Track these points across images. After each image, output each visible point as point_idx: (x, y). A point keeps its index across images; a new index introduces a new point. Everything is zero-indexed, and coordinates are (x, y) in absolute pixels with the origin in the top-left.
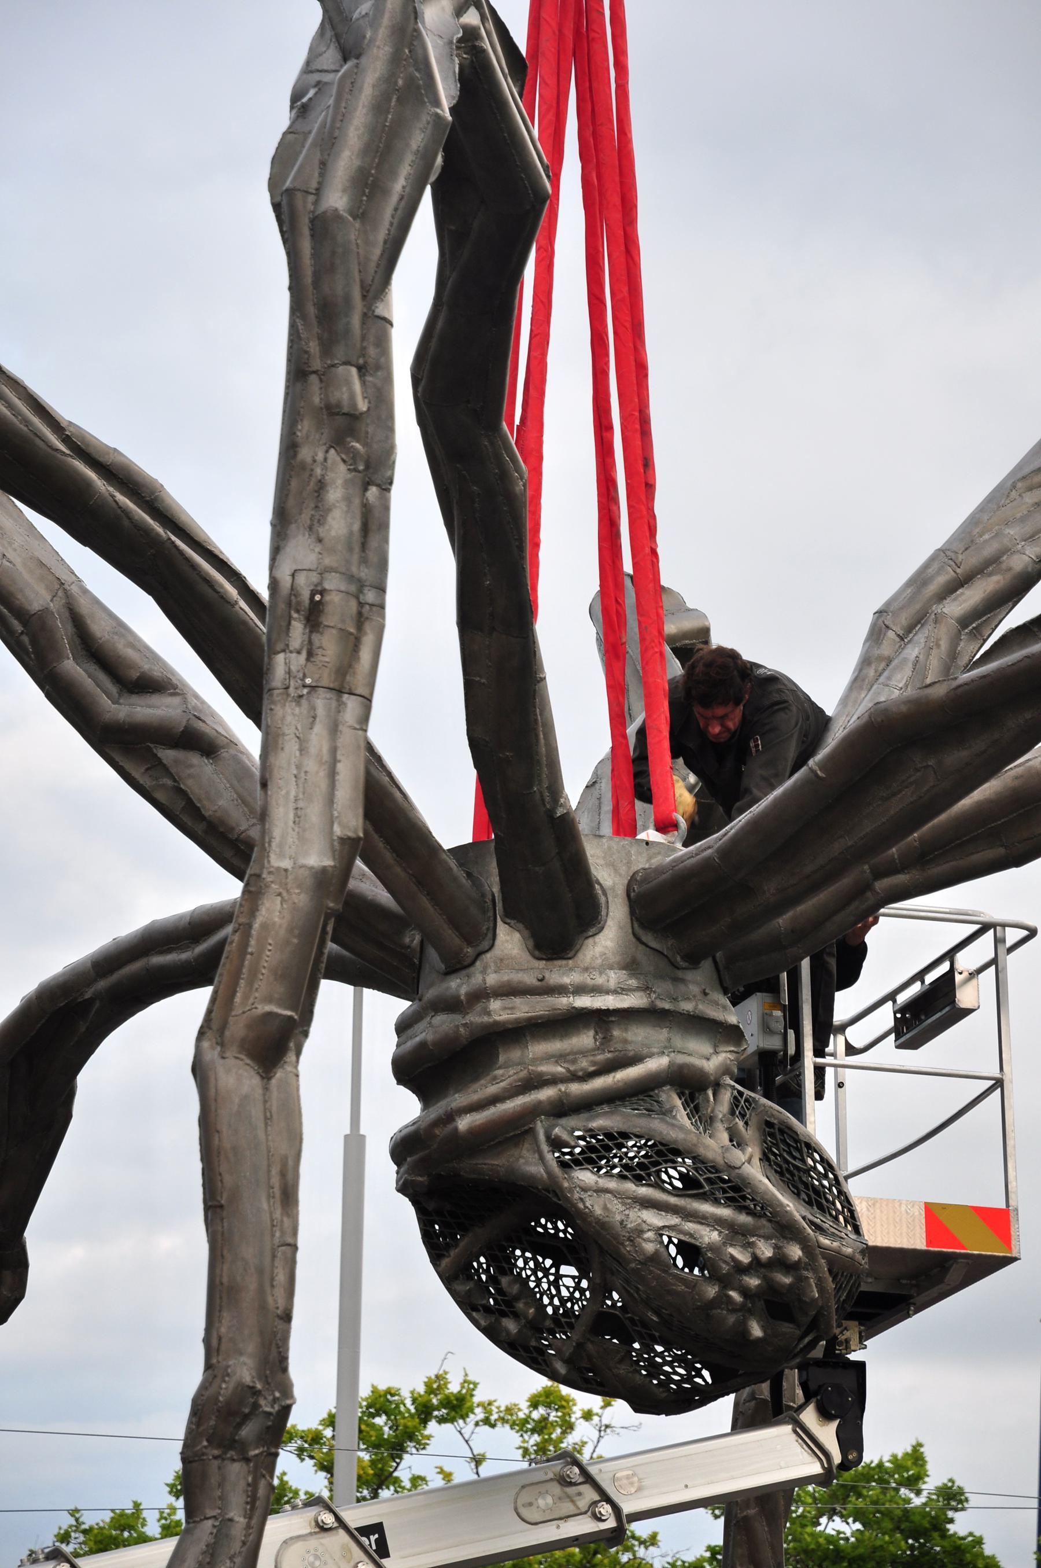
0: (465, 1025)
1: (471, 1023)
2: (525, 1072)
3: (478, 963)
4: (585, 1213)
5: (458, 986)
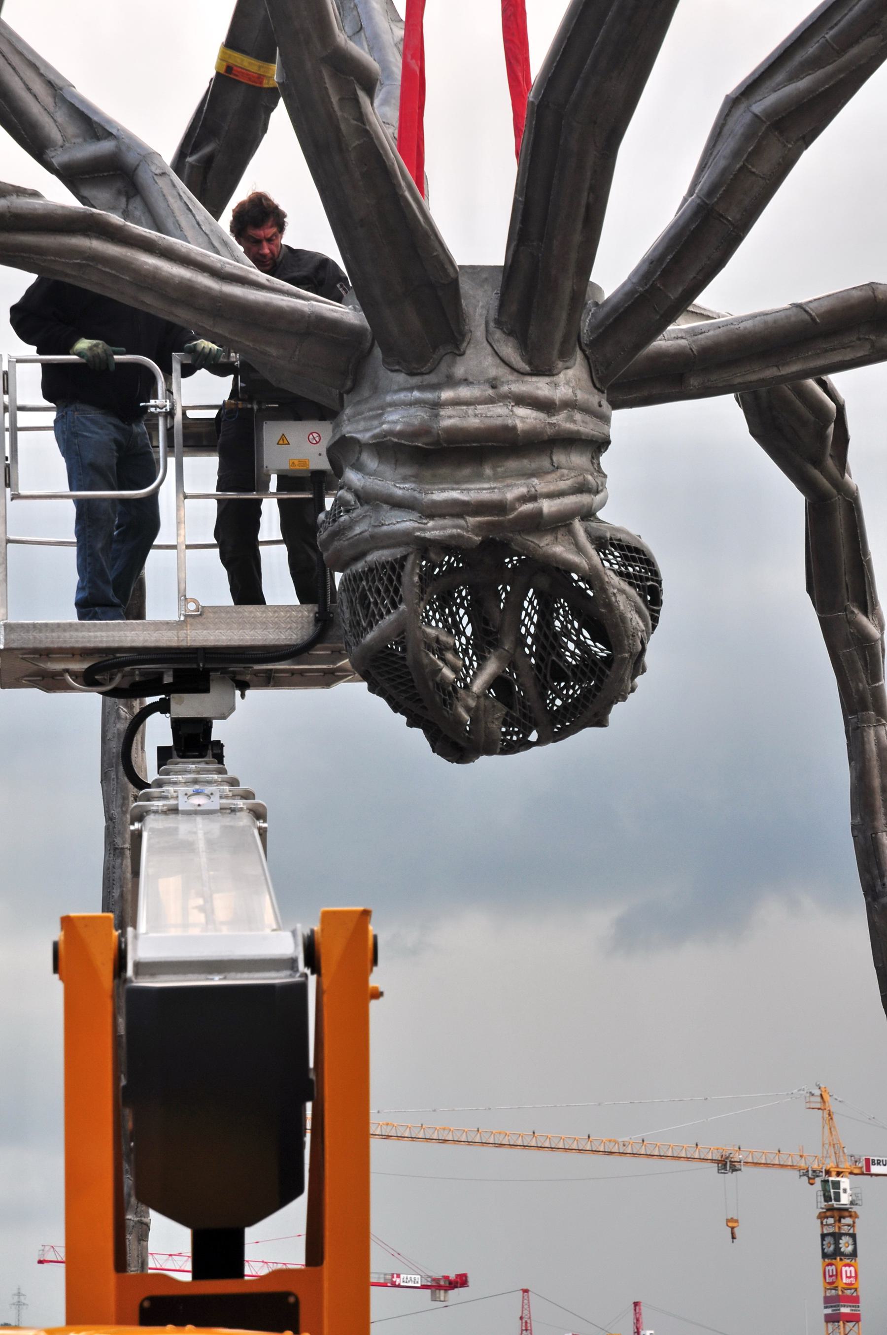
0: (551, 424)
1: (559, 425)
2: (581, 477)
3: (561, 375)
4: (615, 606)
5: (540, 387)
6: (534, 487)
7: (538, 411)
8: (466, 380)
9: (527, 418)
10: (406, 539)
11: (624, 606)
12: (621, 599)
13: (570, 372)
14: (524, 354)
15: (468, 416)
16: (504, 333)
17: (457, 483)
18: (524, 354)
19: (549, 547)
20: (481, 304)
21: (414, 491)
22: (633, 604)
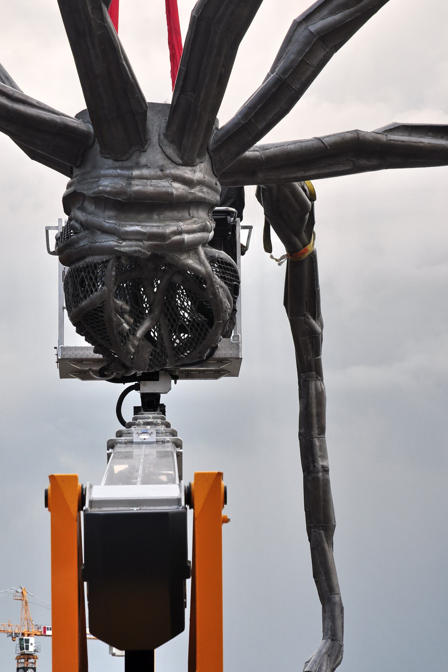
1: (195, 194)
2: (204, 223)
3: (198, 166)
4: (218, 295)
6: (180, 227)
7: (184, 185)
8: (146, 165)
9: (179, 189)
10: (110, 251)
11: (222, 295)
12: (221, 290)
13: (202, 165)
14: (179, 153)
15: (147, 185)
16: (169, 141)
17: (139, 222)
18: (179, 153)
19: (185, 260)
20: (156, 124)
21: (116, 225)
22: (226, 294)
